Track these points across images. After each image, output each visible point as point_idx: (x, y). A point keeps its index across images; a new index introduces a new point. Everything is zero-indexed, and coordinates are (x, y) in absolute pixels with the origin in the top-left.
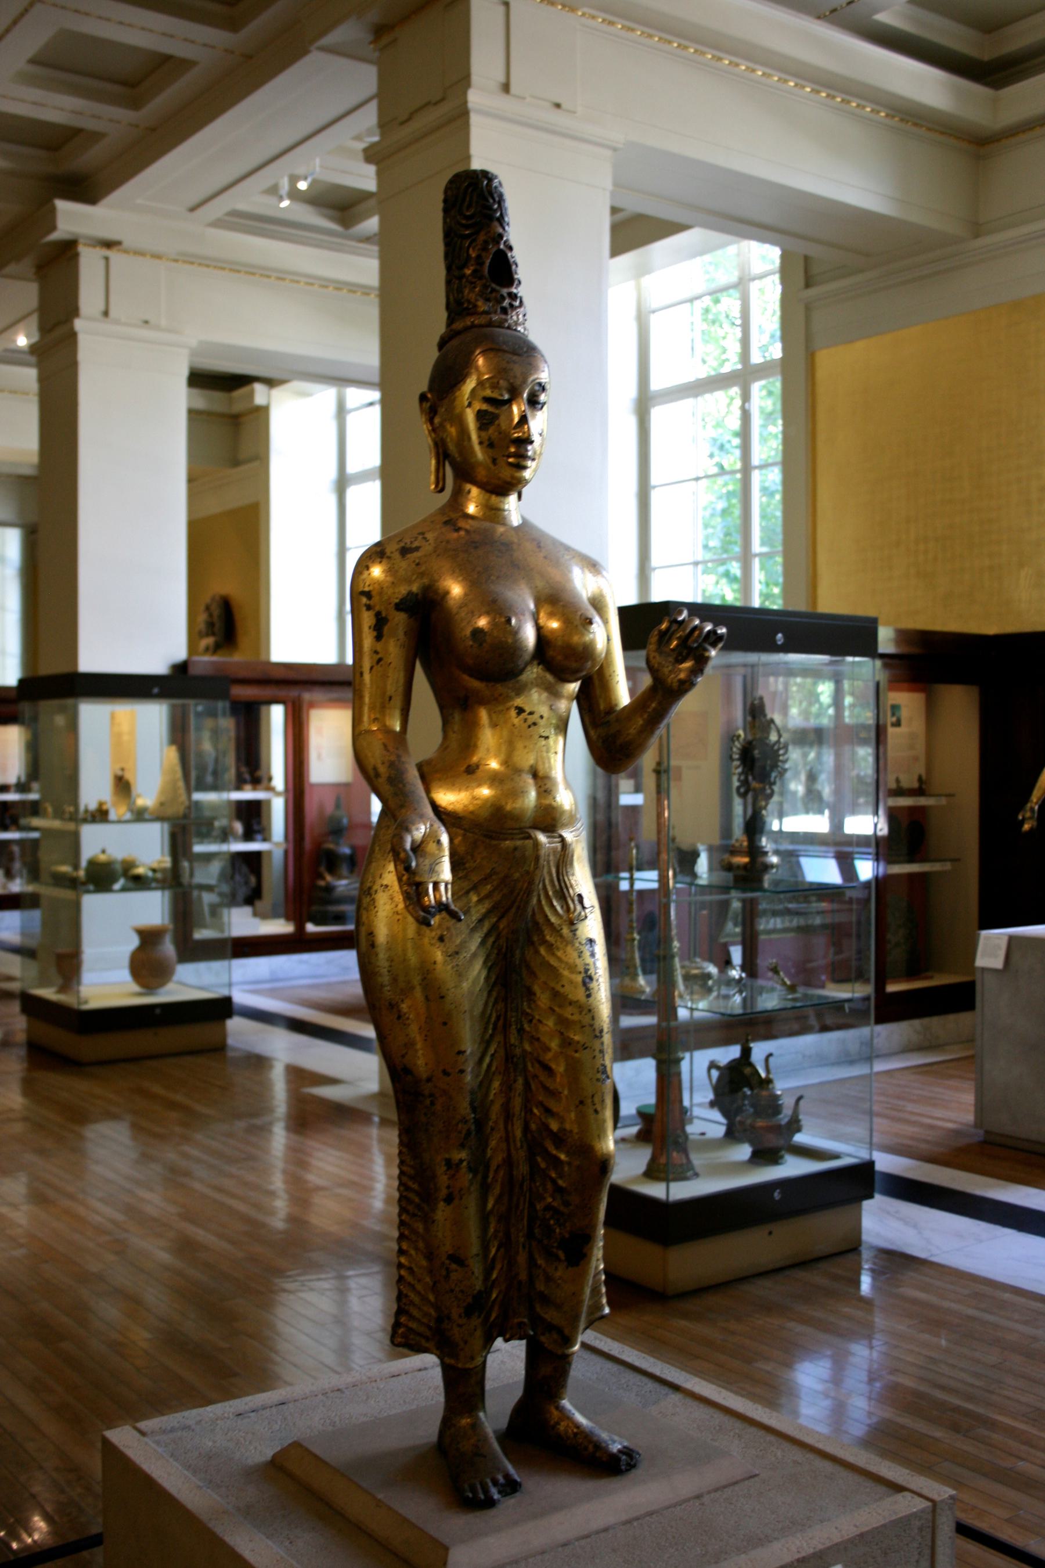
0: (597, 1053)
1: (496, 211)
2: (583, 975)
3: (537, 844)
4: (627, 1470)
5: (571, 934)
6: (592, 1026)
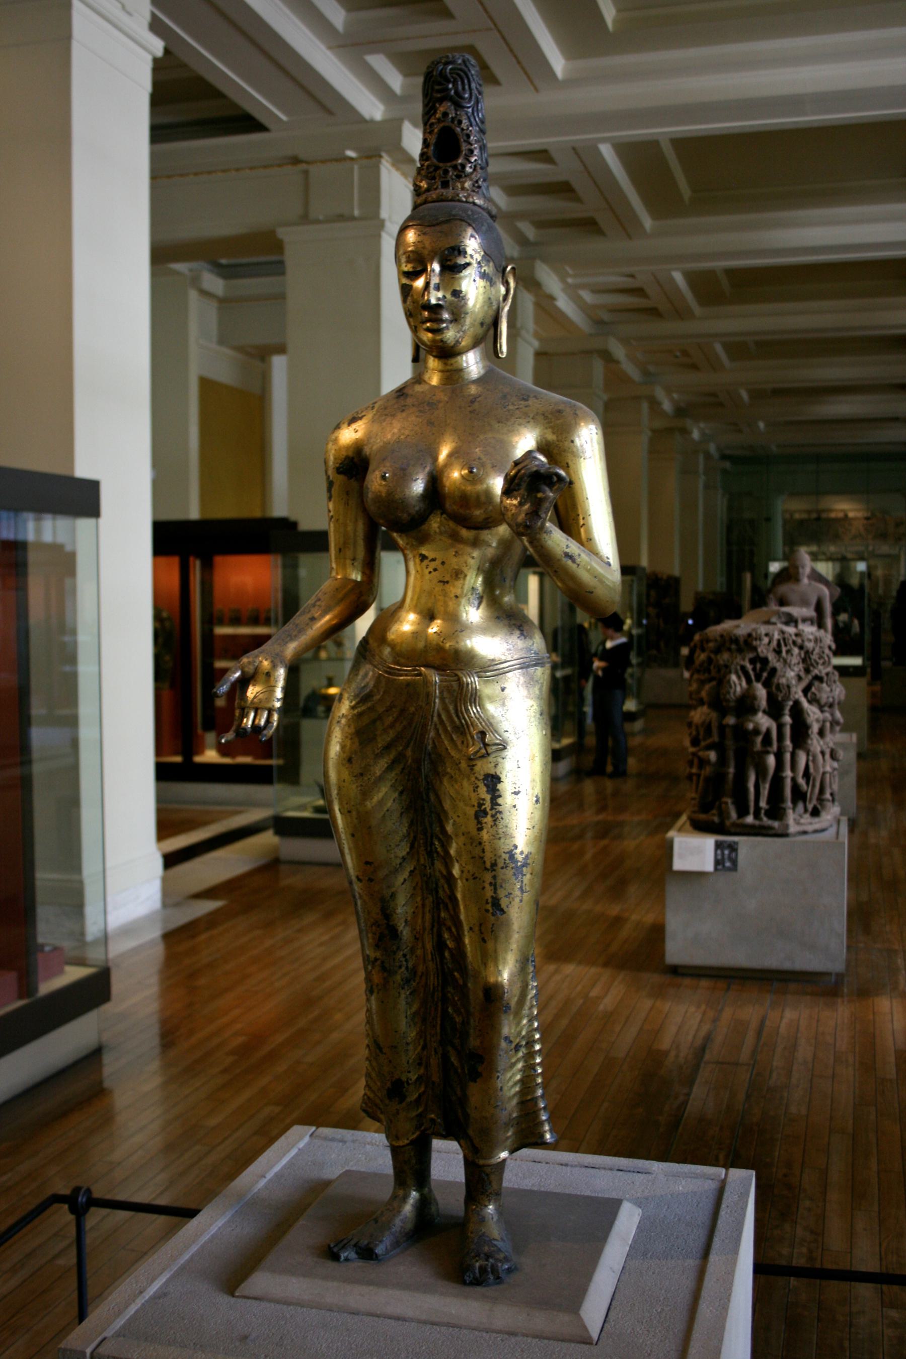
0: (487, 885)
1: (451, 90)
2: (476, 808)
3: (426, 682)
4: (471, 1284)
5: (468, 769)
6: (482, 858)
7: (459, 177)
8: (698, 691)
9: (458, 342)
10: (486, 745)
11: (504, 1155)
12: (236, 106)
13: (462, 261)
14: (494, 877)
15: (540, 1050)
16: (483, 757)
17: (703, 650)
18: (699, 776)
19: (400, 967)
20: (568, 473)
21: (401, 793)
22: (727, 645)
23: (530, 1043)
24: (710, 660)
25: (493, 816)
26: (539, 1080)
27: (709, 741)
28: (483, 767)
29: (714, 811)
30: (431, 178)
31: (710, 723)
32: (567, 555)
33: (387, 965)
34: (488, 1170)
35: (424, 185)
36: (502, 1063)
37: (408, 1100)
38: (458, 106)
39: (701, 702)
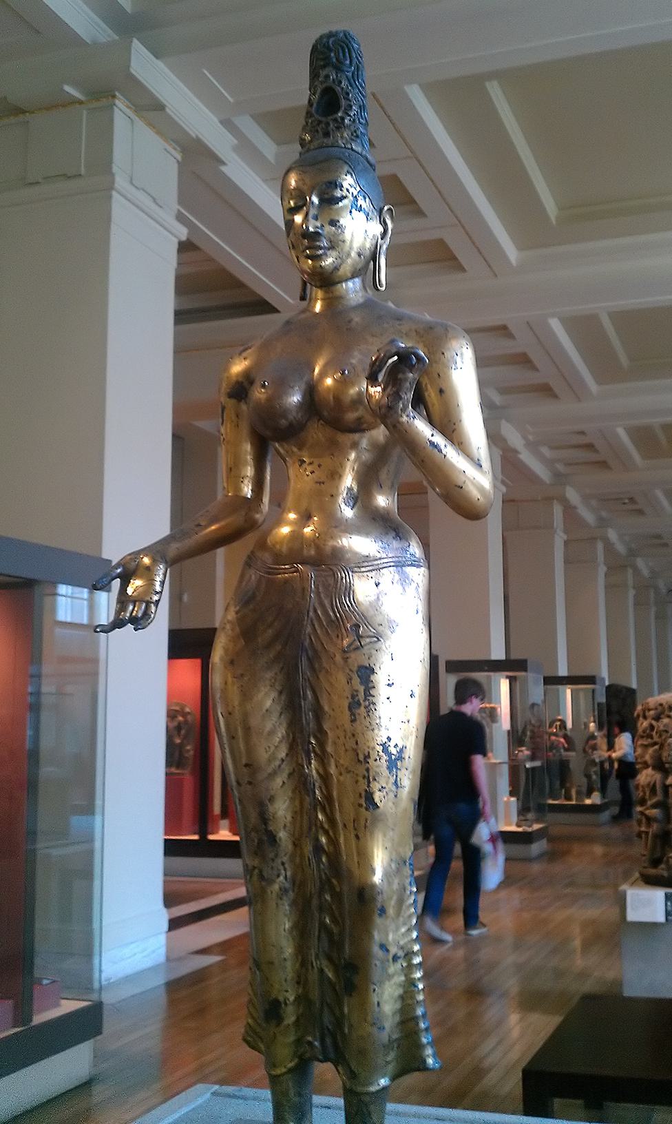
0: (360, 779)
6: (355, 751)
7: (338, 128)
8: (642, 756)
9: (336, 269)
10: (359, 637)
11: (383, 1082)
12: (254, 293)
13: (338, 193)
14: (368, 770)
15: (420, 964)
16: (357, 648)
17: (645, 717)
18: (647, 833)
19: (278, 876)
20: (430, 354)
21: (280, 693)
22: (667, 712)
23: (409, 955)
24: (652, 727)
25: (366, 707)
26: (421, 997)
27: (654, 800)
28: (357, 659)
29: (663, 866)
30: (314, 132)
31: (654, 785)
32: (432, 443)
33: (265, 874)
34: (367, 1099)
35: (308, 137)
36: (376, 974)
37: (286, 1022)
38: (338, 69)
39: (646, 765)
